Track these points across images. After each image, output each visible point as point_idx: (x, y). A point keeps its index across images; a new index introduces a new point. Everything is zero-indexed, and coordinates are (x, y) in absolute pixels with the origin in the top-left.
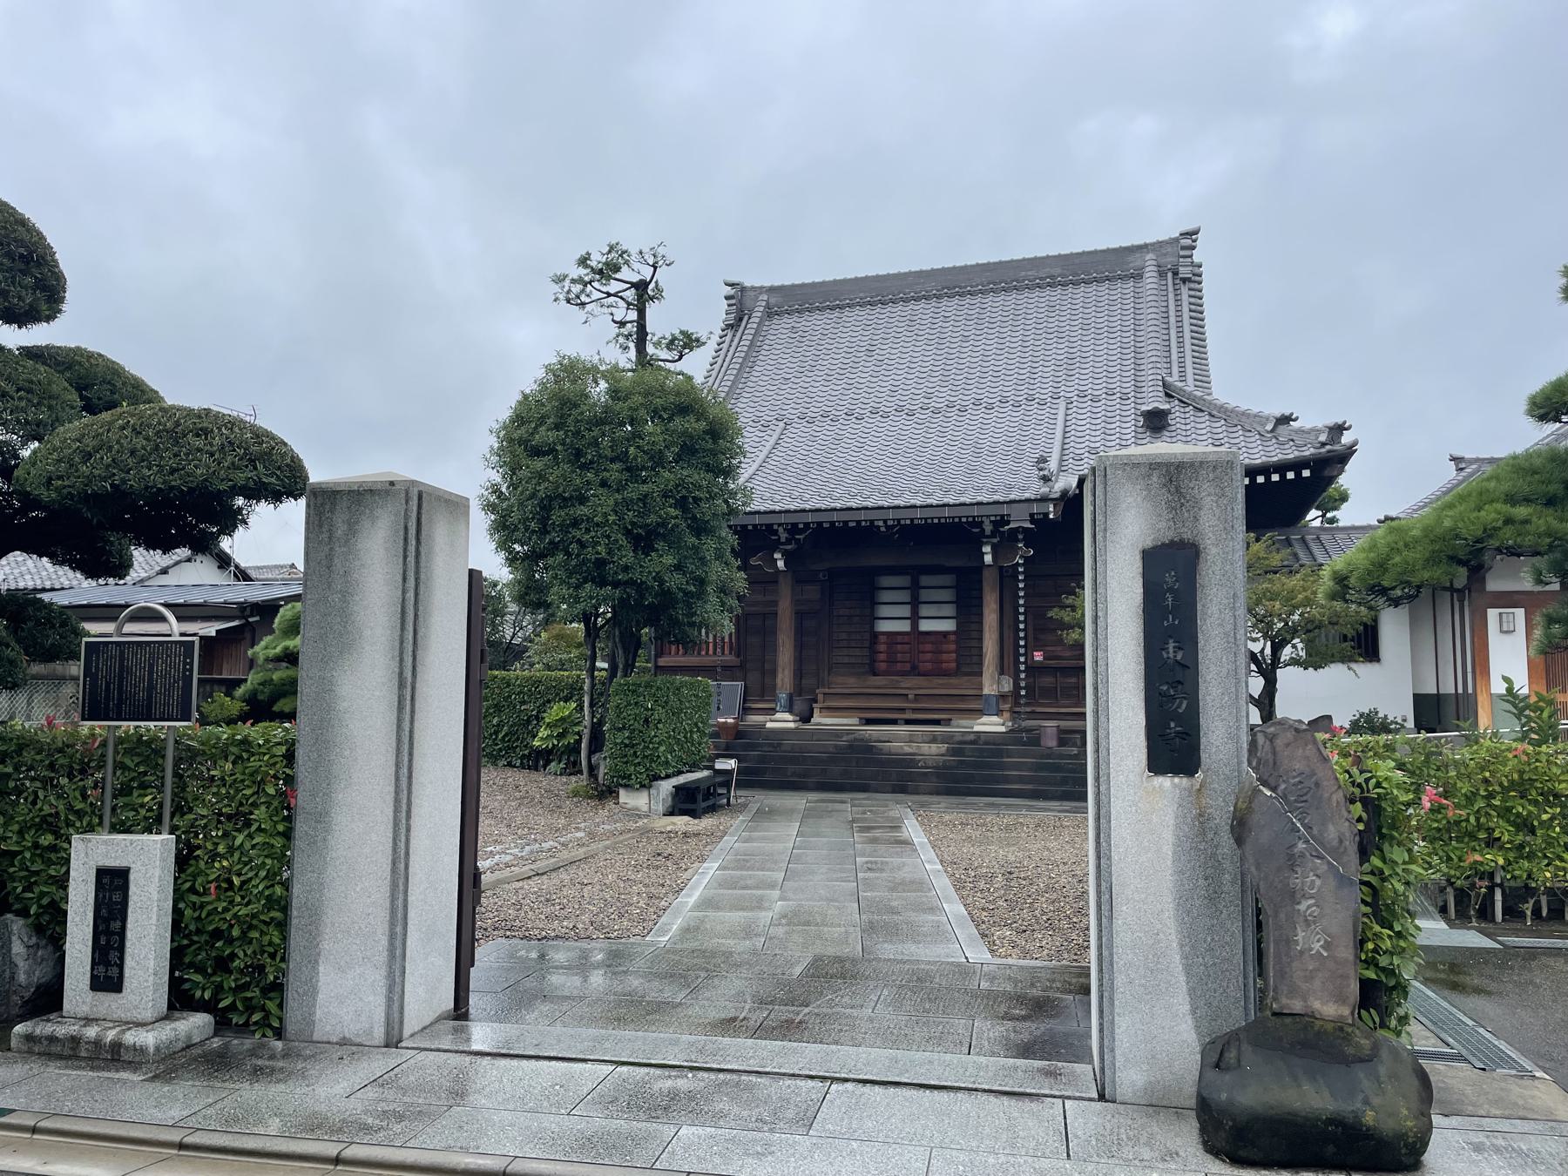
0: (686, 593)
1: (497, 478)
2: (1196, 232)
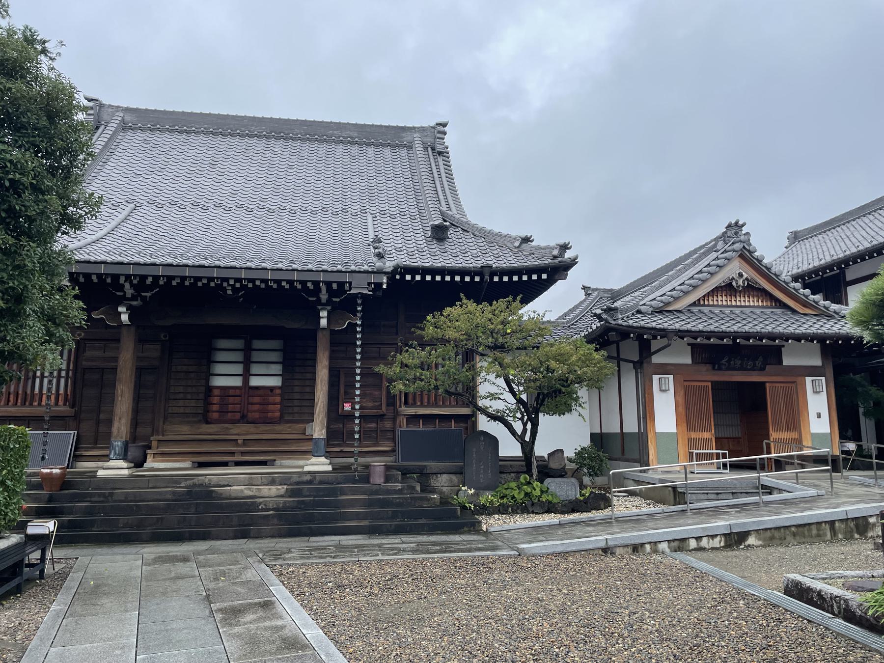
2: (444, 125)
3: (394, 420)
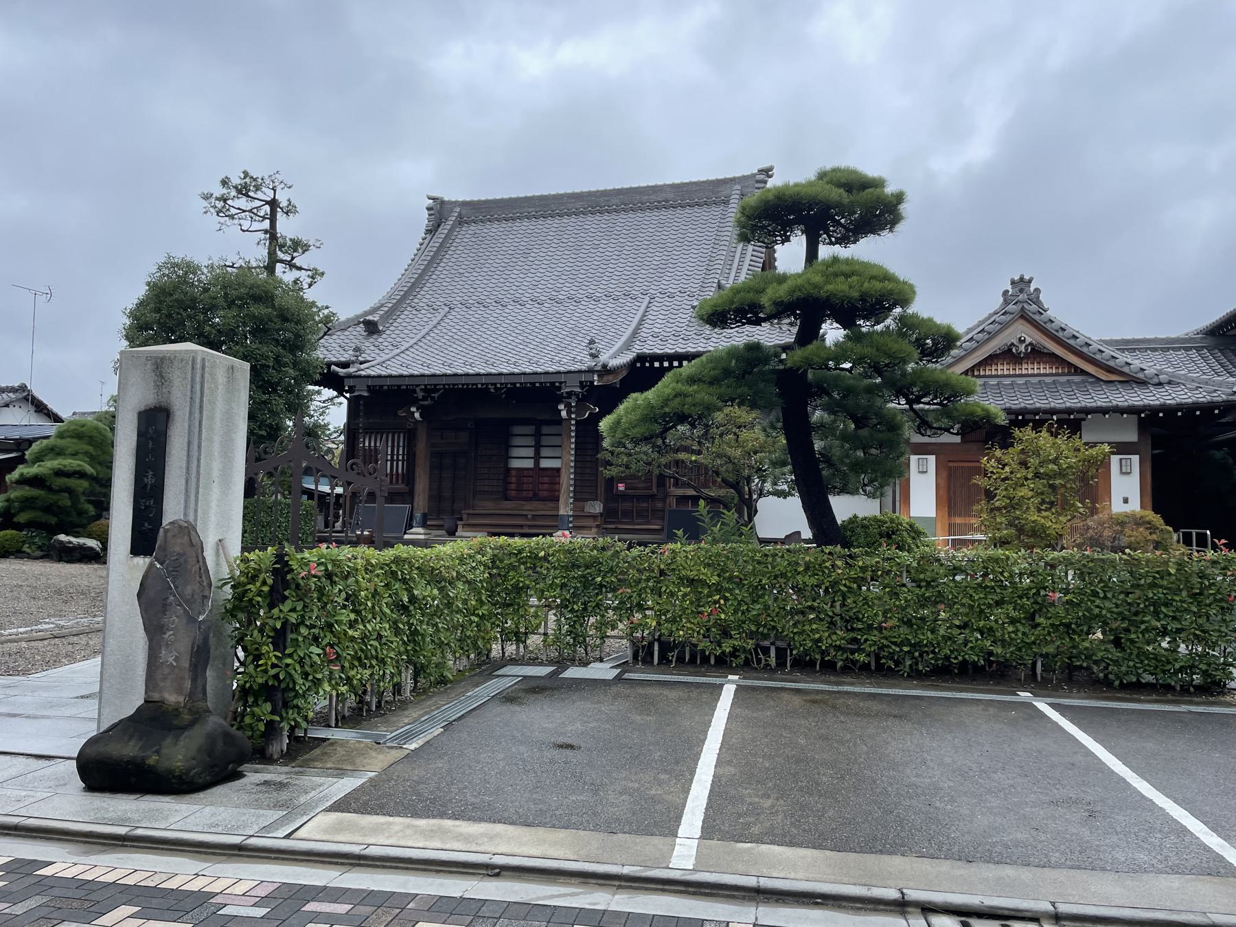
3: (664, 500)
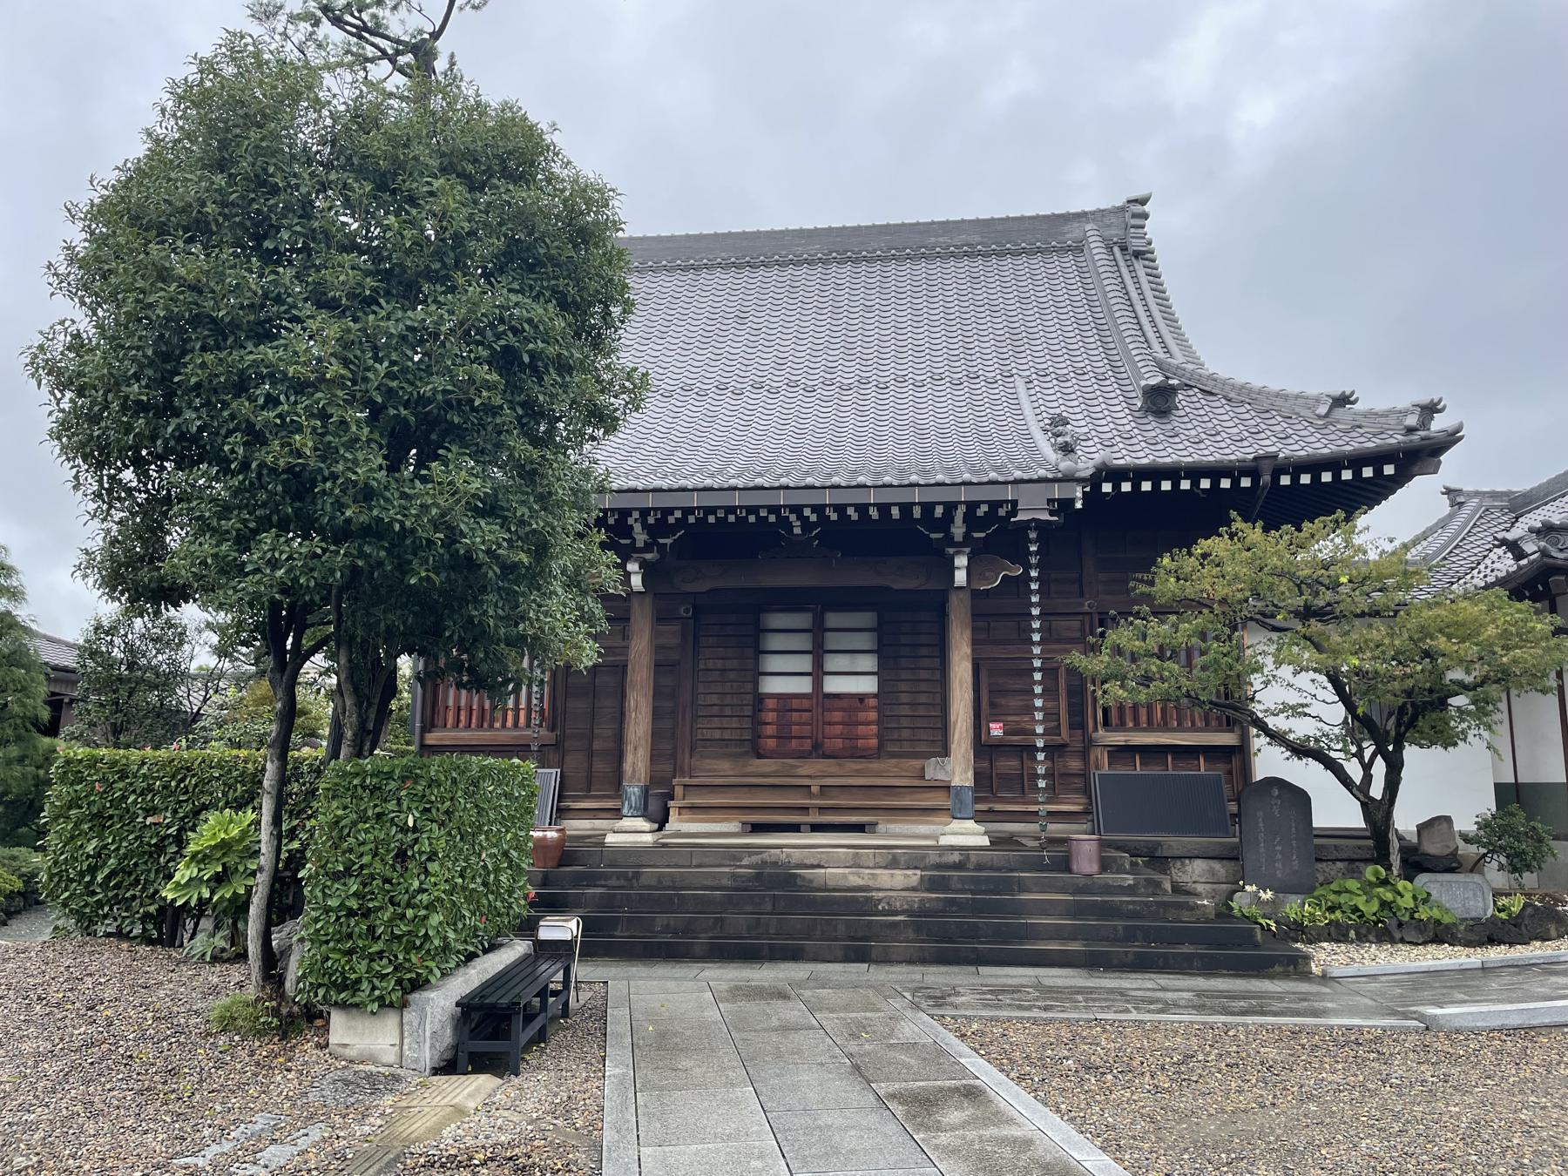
0: (509, 569)
1: (85, 324)
3: (1084, 754)
